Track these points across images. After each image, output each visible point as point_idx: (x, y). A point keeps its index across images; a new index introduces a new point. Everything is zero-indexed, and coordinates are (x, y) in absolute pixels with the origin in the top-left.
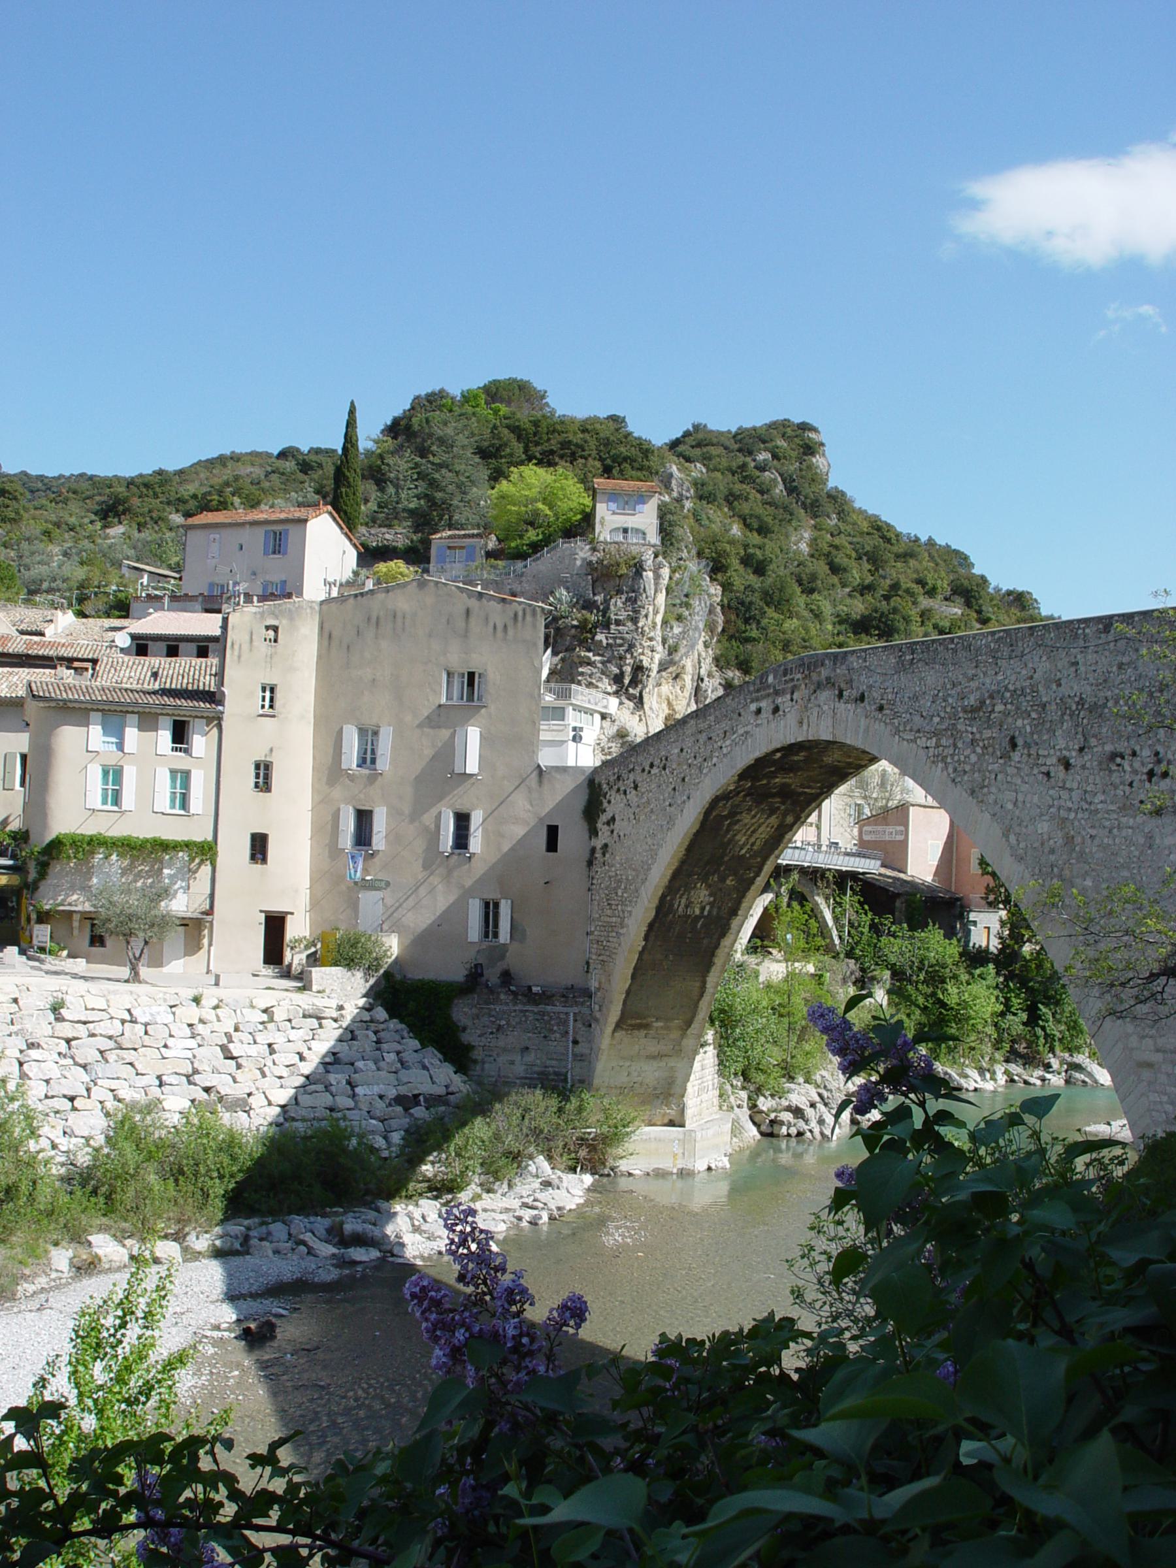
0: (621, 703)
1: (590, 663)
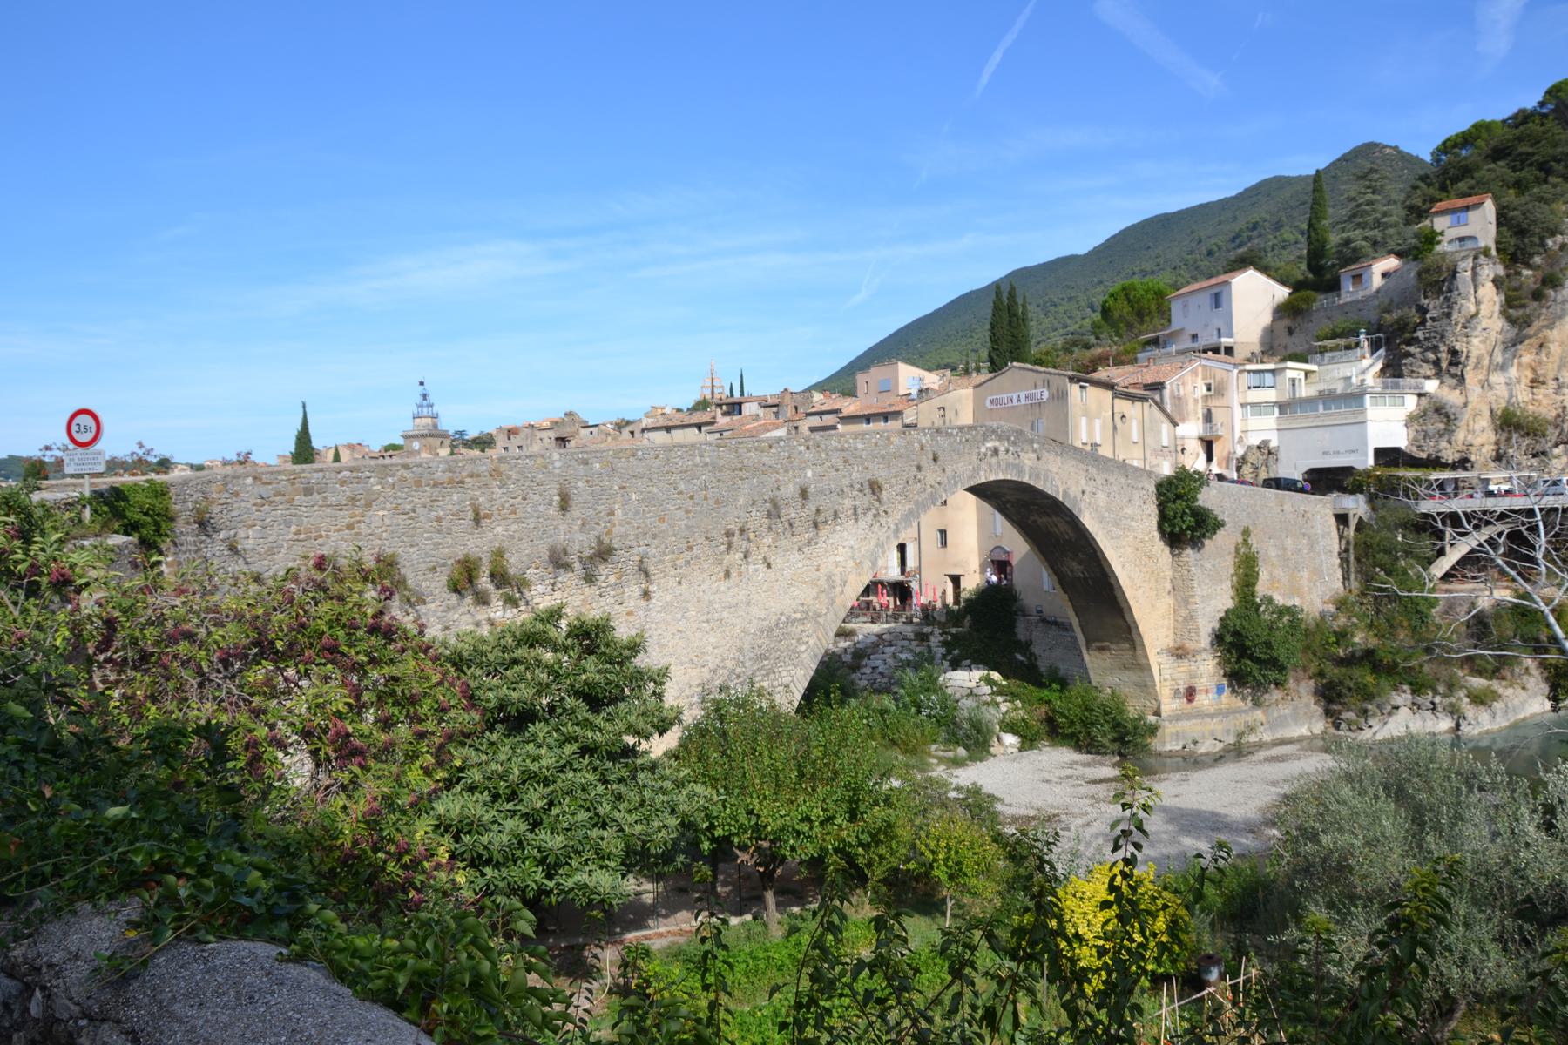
0: (1442, 383)
1: (1408, 355)
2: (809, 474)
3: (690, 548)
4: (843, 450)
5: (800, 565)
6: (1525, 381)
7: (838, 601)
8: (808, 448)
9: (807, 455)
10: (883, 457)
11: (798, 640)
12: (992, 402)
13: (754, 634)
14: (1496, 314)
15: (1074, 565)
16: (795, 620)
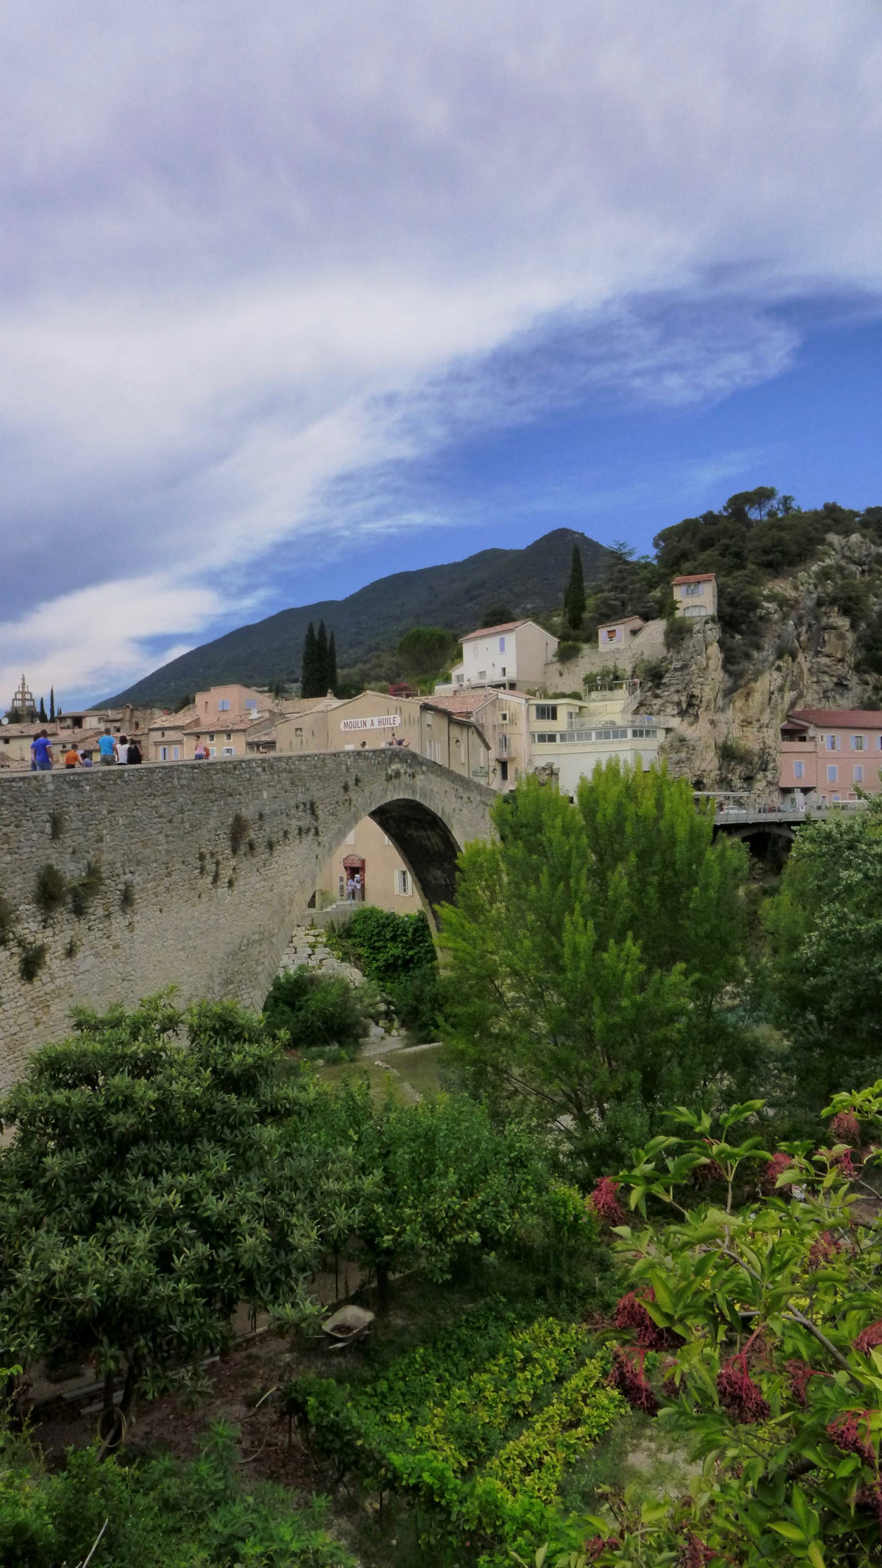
2: (265, 795)
3: (169, 875)
4: (290, 772)
5: (258, 886)
6: (738, 721)
7: (287, 919)
8: (264, 770)
9: (264, 777)
10: (320, 778)
11: (257, 961)
12: (346, 725)
13: (222, 959)
14: (720, 668)
15: (438, 873)
16: (255, 942)
